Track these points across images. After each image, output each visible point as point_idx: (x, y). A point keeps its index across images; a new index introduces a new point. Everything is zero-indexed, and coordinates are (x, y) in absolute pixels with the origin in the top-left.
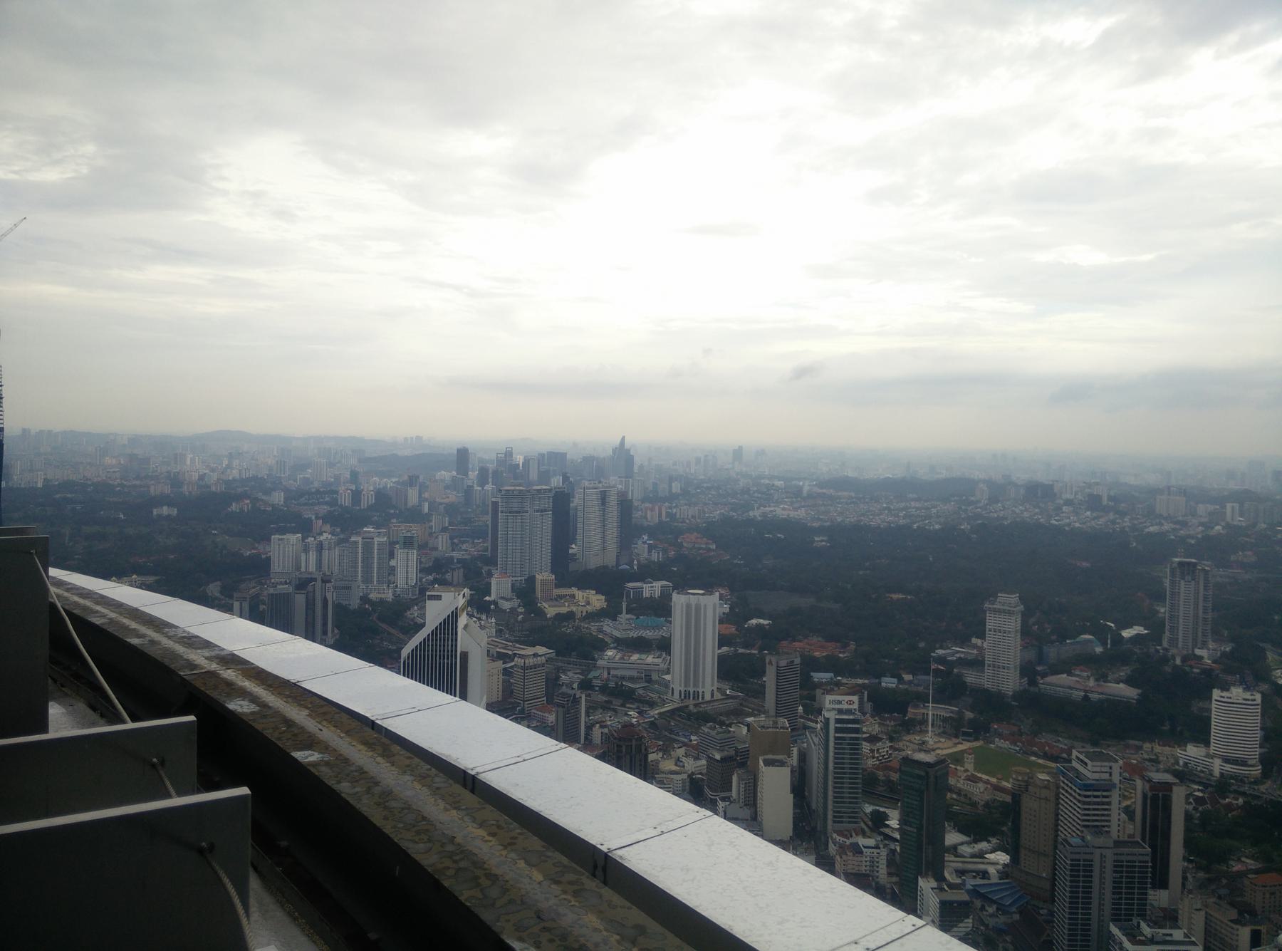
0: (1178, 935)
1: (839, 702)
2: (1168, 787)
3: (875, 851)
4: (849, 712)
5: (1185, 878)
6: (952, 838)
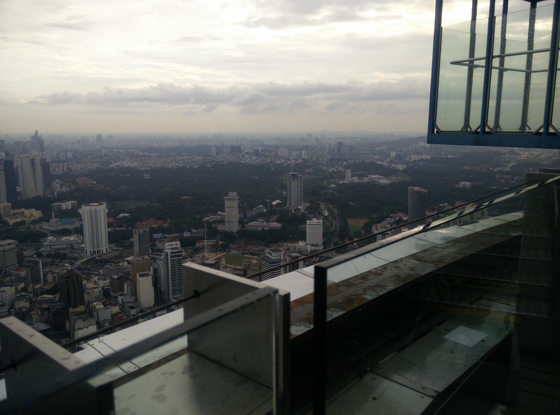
1: (172, 245)
4: (176, 248)
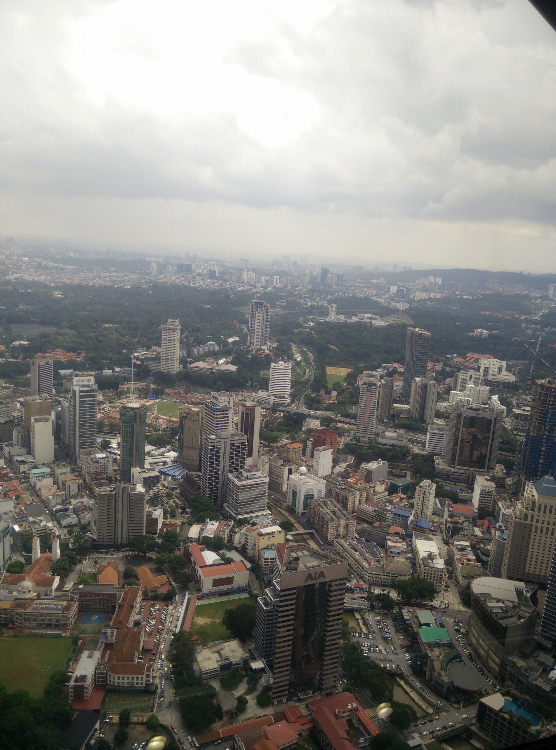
0: (259, 474)
1: (82, 381)
2: (253, 408)
3: (106, 460)
5: (259, 451)
6: (148, 448)
